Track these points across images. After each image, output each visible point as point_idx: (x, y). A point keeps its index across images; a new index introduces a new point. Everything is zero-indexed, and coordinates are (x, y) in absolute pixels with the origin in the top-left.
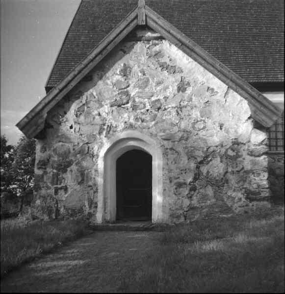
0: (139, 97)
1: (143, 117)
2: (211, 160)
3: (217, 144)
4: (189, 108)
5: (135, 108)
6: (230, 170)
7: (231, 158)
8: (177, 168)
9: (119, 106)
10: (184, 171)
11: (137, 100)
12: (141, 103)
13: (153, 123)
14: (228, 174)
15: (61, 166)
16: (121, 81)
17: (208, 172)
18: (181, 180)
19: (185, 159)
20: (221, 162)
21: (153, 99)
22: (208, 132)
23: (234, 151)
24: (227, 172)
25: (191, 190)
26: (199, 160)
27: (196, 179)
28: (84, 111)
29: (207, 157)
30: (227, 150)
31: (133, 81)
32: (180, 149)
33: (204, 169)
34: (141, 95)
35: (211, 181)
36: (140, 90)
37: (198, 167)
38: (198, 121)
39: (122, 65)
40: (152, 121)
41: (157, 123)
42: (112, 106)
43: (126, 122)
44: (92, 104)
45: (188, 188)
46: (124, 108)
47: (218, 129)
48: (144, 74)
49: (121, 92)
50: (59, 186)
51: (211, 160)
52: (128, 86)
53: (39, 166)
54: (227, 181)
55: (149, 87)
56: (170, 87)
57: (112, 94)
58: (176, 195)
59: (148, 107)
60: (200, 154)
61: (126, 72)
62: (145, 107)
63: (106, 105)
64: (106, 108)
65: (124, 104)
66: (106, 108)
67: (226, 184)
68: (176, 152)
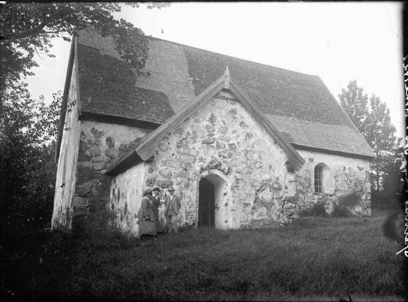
0: (221, 139)
1: (224, 154)
2: (264, 189)
3: (268, 179)
4: (252, 152)
5: (218, 146)
6: (275, 196)
7: (275, 189)
8: (243, 193)
9: (208, 144)
10: (249, 195)
11: (220, 141)
12: (223, 144)
13: (230, 159)
14: (274, 200)
15: (165, 184)
16: (209, 126)
17: (262, 197)
18: (247, 202)
19: (249, 187)
20: (270, 191)
21: (231, 142)
22: (263, 170)
23: (277, 184)
24: (273, 198)
26: (257, 188)
28: (183, 144)
29: (262, 187)
30: (273, 183)
31: (217, 128)
32: (246, 180)
33: (260, 195)
34: (222, 138)
35: (264, 204)
36: (223, 135)
37: (256, 194)
38: (257, 162)
39: (211, 114)
40: (229, 158)
41: (232, 160)
42: (203, 143)
43: (212, 157)
44: (189, 139)
45: (251, 208)
46: (211, 146)
47: (269, 168)
49: (209, 135)
51: (264, 189)
52: (213, 131)
53: (148, 184)
54: (273, 204)
55: (228, 133)
56: (241, 135)
57: (203, 134)
58: (244, 211)
59: (227, 147)
61: (212, 119)
62: (225, 148)
63: (199, 142)
64: (198, 145)
65: (211, 143)
66: (198, 145)
67: (273, 206)
68: (244, 182)
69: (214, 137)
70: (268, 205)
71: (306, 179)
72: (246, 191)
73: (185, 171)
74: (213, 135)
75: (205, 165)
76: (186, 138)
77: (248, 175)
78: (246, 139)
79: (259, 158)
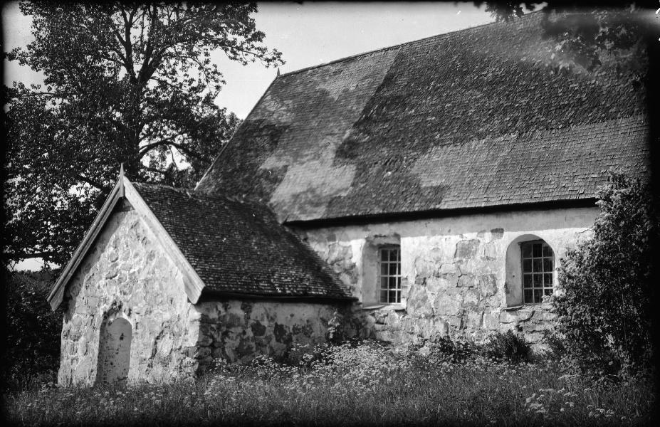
24: (172, 350)
25: (149, 366)
26: (157, 335)
27: (153, 356)
32: (146, 324)
37: (156, 343)
42: (106, 279)
48: (127, 246)
50: (74, 356)
52: (117, 259)
60: (158, 329)
66: (103, 282)
69: (117, 267)
70: (165, 362)
71: (484, 278)
72: (145, 340)
73: (92, 317)
74: (117, 265)
75: (108, 307)
76: (93, 275)
77: (148, 316)
78: (147, 263)
79: (161, 289)
